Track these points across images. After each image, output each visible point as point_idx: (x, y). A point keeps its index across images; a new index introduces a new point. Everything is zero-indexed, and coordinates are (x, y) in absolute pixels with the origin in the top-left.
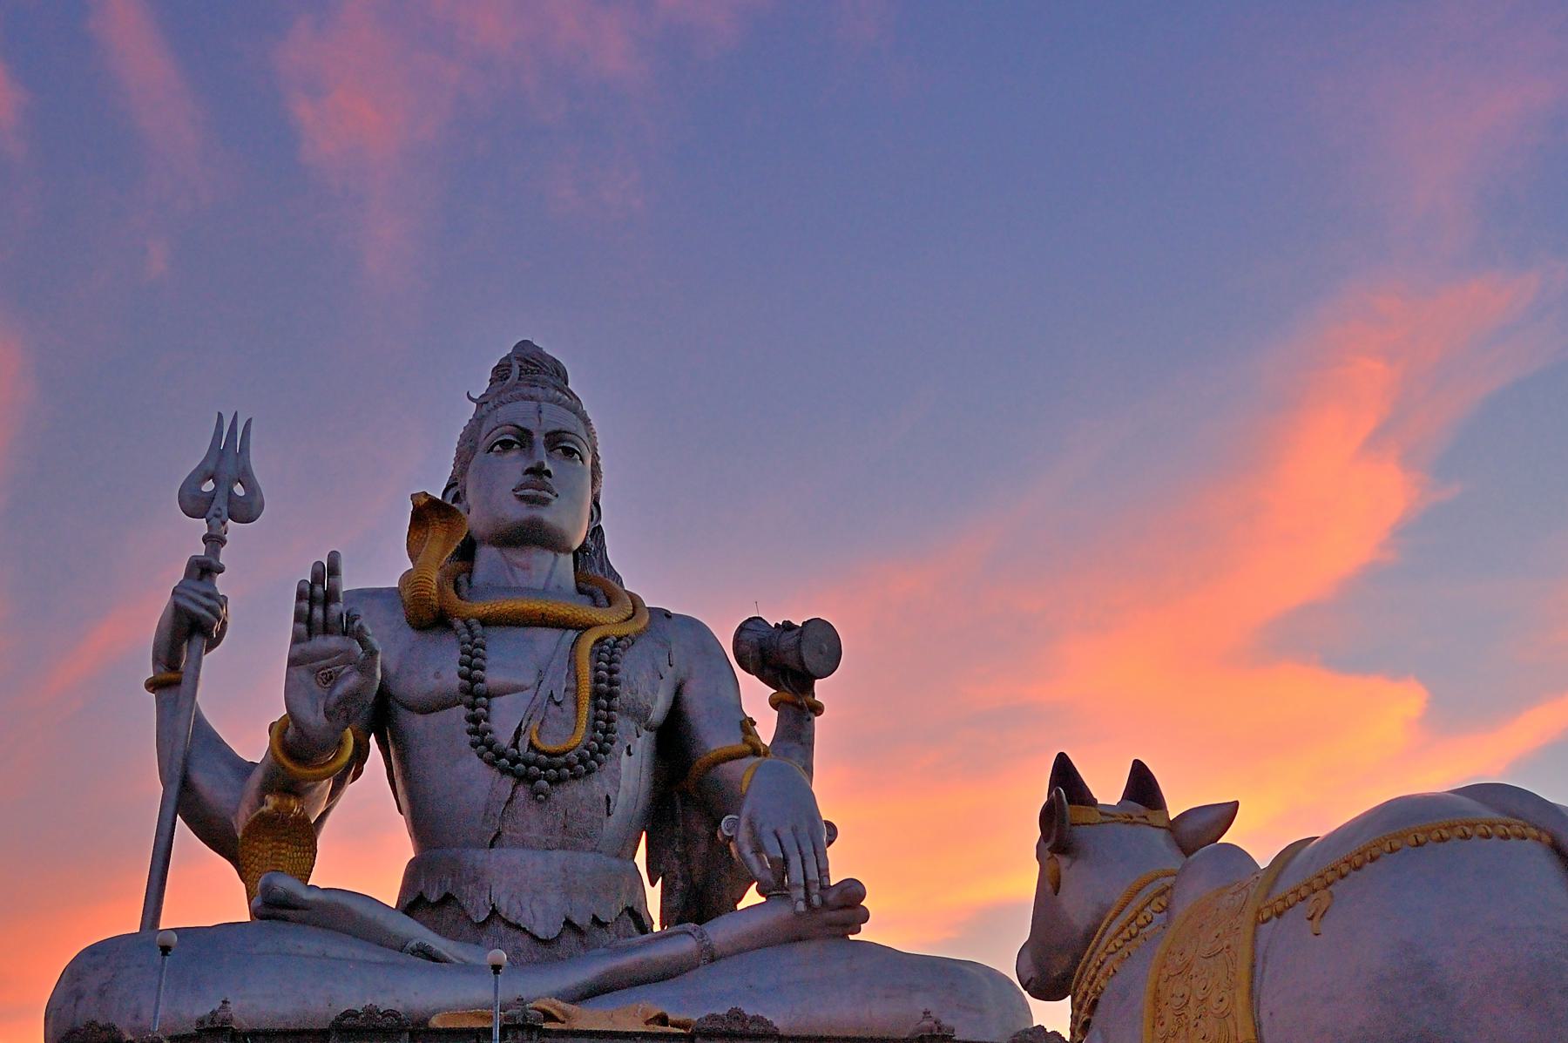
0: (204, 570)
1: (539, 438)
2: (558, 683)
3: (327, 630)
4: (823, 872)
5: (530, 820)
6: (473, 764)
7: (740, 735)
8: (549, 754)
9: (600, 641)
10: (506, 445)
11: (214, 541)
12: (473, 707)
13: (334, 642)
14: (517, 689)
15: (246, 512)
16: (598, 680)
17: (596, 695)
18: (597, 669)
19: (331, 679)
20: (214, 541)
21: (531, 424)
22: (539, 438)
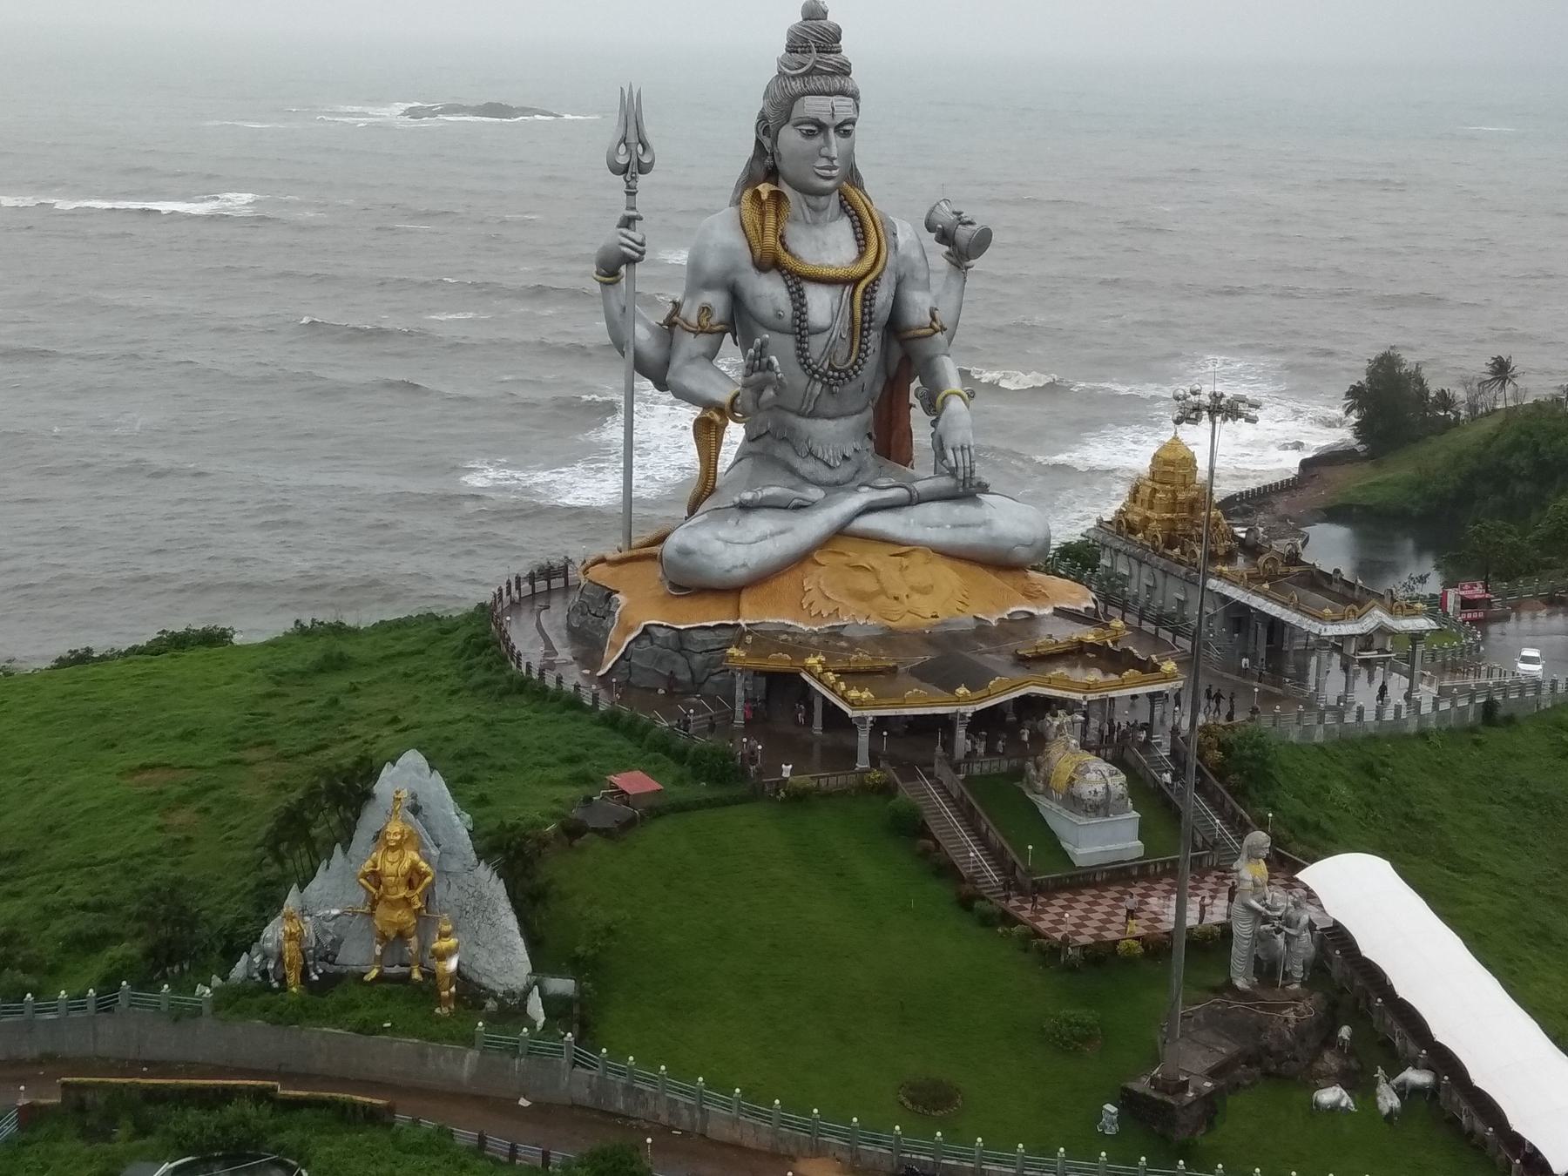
0: (628, 222)
1: (831, 131)
2: (841, 326)
3: (760, 369)
4: (972, 472)
5: (830, 405)
6: (798, 370)
7: (929, 319)
8: (839, 371)
9: (865, 291)
10: (809, 135)
11: (631, 193)
12: (800, 342)
13: (759, 375)
14: (822, 331)
15: (643, 169)
16: (863, 322)
17: (862, 329)
18: (863, 314)
19: (760, 391)
20: (631, 193)
21: (825, 119)
22: (831, 131)
